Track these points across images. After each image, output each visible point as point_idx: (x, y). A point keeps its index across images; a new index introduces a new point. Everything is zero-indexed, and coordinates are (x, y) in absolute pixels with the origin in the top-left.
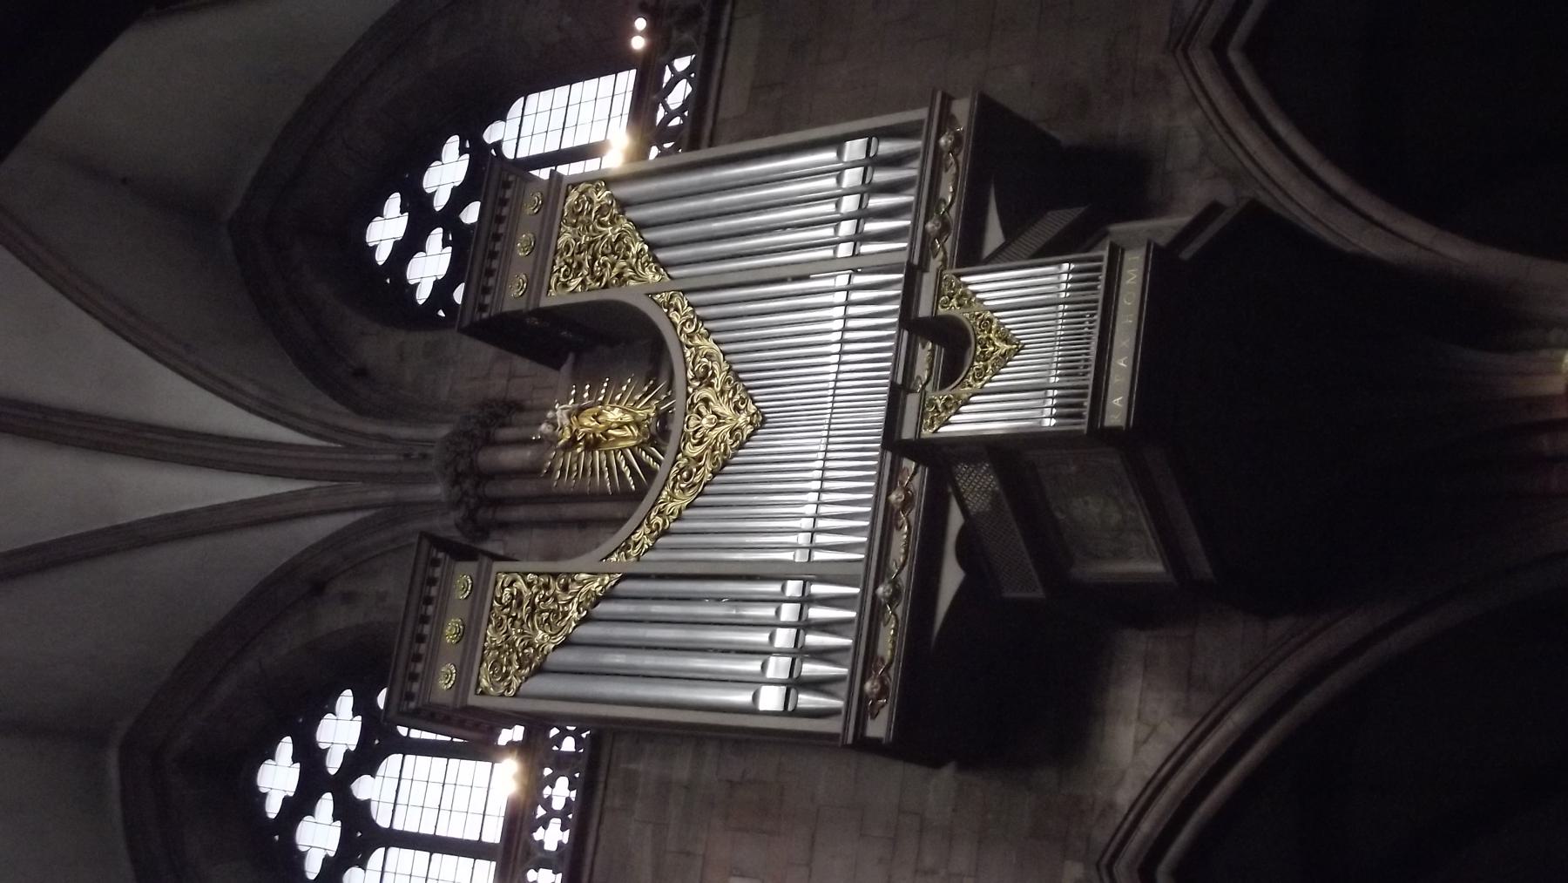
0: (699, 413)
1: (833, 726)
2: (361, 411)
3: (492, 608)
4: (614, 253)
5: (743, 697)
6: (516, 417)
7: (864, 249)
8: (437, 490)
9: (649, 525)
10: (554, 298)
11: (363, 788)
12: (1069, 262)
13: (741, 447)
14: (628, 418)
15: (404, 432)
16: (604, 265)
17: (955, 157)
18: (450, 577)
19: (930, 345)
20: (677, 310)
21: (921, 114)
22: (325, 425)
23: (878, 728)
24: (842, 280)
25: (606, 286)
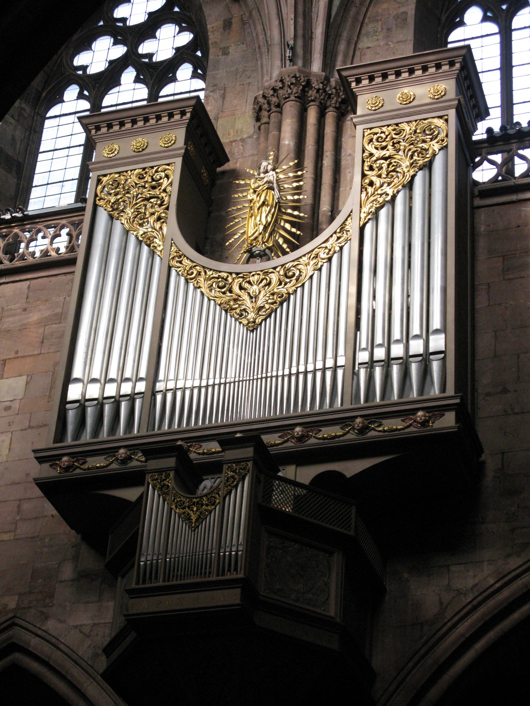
3: (152, 167)
18: (176, 126)
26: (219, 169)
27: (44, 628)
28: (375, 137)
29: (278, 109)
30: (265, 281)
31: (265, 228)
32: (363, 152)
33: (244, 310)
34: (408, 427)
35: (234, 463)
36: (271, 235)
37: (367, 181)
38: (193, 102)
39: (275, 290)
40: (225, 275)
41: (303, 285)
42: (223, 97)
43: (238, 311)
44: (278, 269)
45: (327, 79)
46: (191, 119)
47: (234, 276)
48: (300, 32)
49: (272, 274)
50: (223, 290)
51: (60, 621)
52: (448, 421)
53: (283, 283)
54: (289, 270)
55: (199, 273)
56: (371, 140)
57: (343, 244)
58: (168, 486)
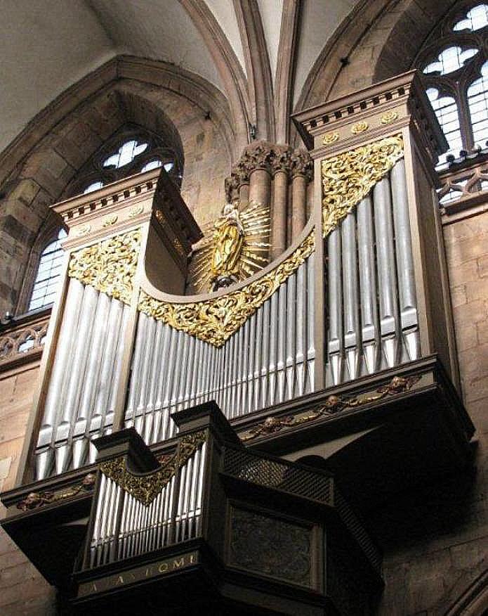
26: (195, 247)
28: (334, 165)
29: (246, 182)
30: (231, 303)
31: (230, 257)
32: (323, 178)
33: (212, 330)
34: (384, 396)
35: (189, 434)
36: (235, 263)
37: (328, 200)
38: (158, 173)
39: (242, 308)
40: (191, 306)
41: (270, 299)
42: (199, 192)
43: (205, 333)
44: (243, 290)
45: (291, 150)
46: (158, 189)
47: (201, 304)
48: (262, 116)
49: (238, 295)
50: (190, 318)
52: (428, 380)
53: (249, 300)
54: (255, 288)
55: (167, 310)
56: (330, 168)
57: (307, 256)
58: (121, 470)
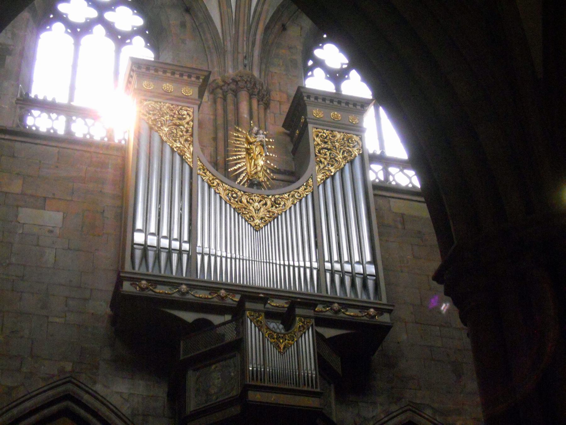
0: (261, 201)
1: (128, 267)
2: (267, 28)
3: (178, 106)
4: (331, 158)
5: (139, 224)
6: (262, 106)
7: (328, 275)
8: (231, 72)
9: (213, 179)
10: (312, 130)
11: (99, 29)
12: (316, 374)
13: (246, 221)
14: (259, 168)
15: (257, 52)
16: (326, 154)
17: (365, 315)
18: (191, 84)
19: (286, 306)
20: (305, 189)
21: (384, 301)
22: (260, 14)
23: (127, 287)
24: (315, 265)
25: (316, 156)
27: (94, 389)
44: (270, 197)
51: (105, 386)
55: (218, 184)
